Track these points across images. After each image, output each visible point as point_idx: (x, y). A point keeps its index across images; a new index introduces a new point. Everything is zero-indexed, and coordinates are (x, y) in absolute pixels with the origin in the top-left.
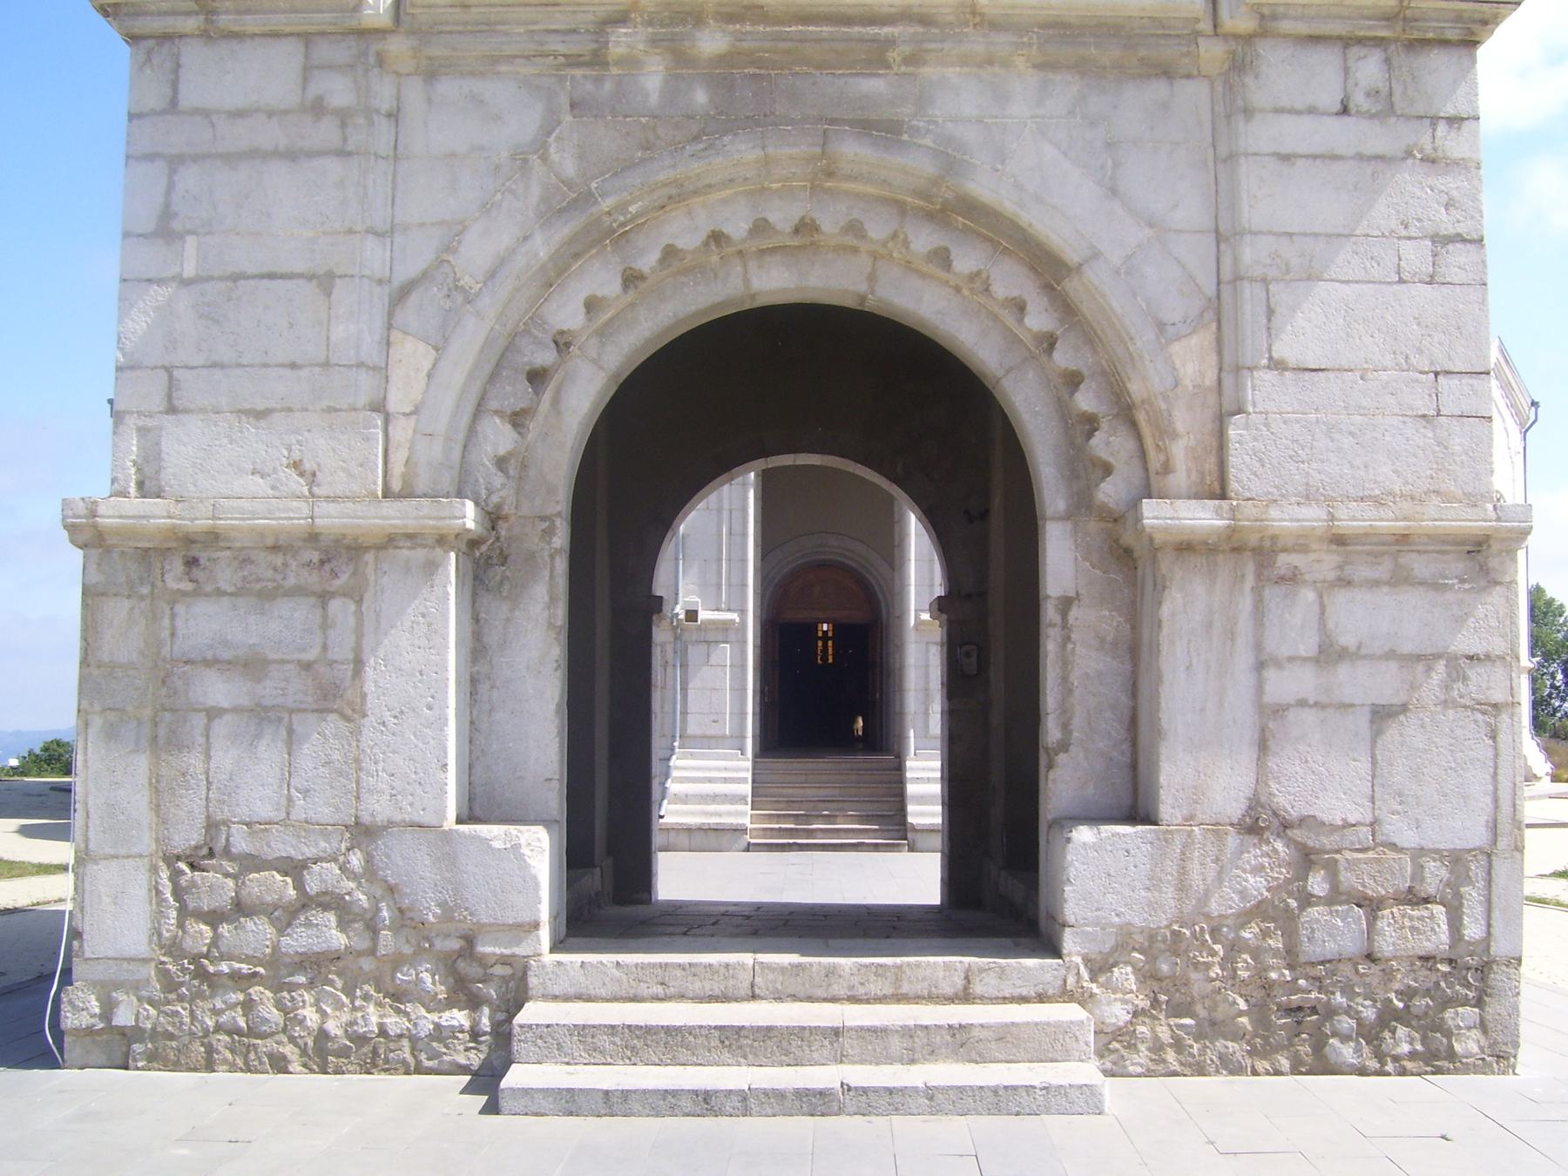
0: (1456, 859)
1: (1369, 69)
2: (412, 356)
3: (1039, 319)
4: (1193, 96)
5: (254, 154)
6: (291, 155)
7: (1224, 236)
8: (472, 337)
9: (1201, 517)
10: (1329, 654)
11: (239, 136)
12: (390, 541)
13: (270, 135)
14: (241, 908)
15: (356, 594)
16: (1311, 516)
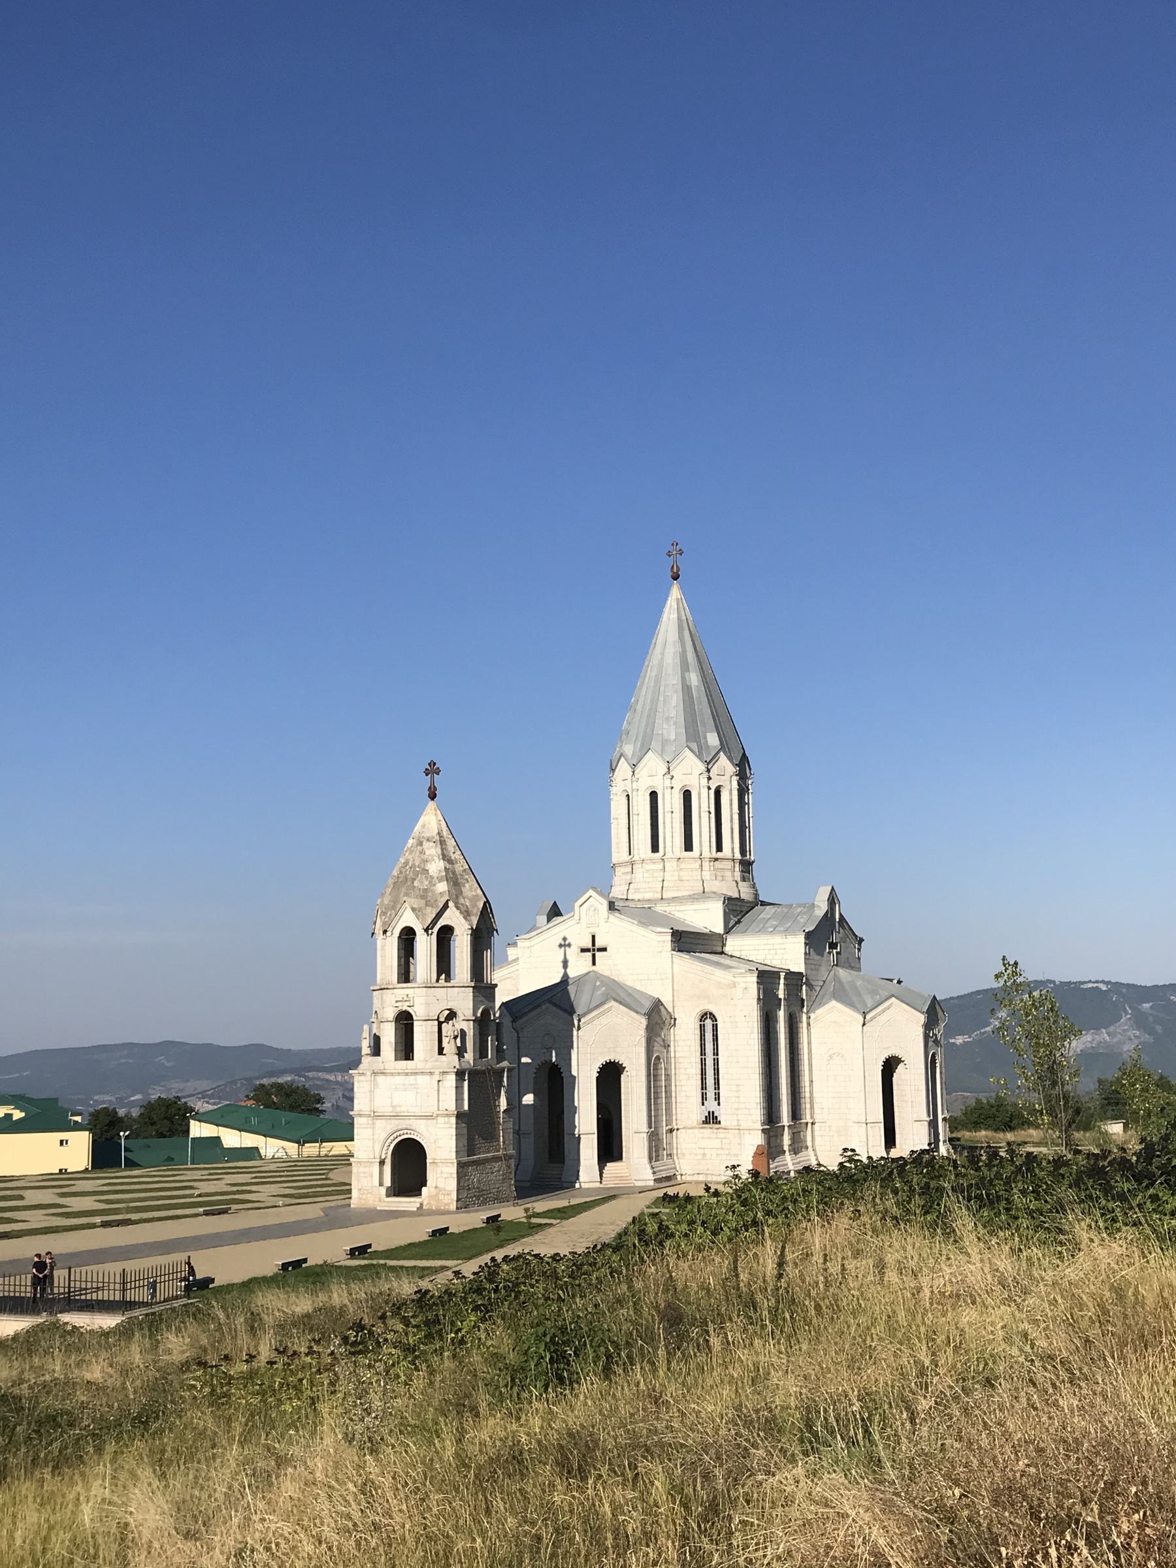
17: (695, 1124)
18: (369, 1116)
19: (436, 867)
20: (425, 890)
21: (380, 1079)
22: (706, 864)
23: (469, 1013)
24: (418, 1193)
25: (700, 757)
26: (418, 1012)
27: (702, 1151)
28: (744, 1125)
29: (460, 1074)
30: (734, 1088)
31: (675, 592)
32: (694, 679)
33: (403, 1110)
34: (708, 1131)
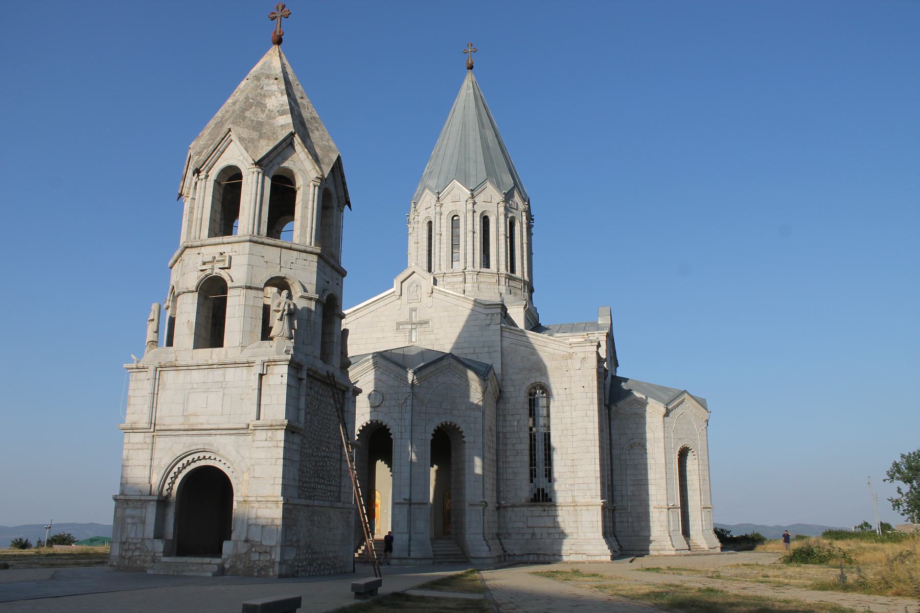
0: (271, 547)
1: (270, 433)
4: (250, 438)
8: (162, 472)
13: (140, 446)
16: (254, 499)
17: (523, 501)
19: (278, 100)
20: (260, 124)
21: (169, 377)
22: (503, 280)
23: (312, 291)
24: (218, 552)
25: (498, 186)
26: (236, 276)
27: (531, 531)
28: (581, 500)
29: (294, 366)
30: (569, 463)
31: (469, 81)
32: (490, 134)
33: (203, 421)
34: (537, 510)
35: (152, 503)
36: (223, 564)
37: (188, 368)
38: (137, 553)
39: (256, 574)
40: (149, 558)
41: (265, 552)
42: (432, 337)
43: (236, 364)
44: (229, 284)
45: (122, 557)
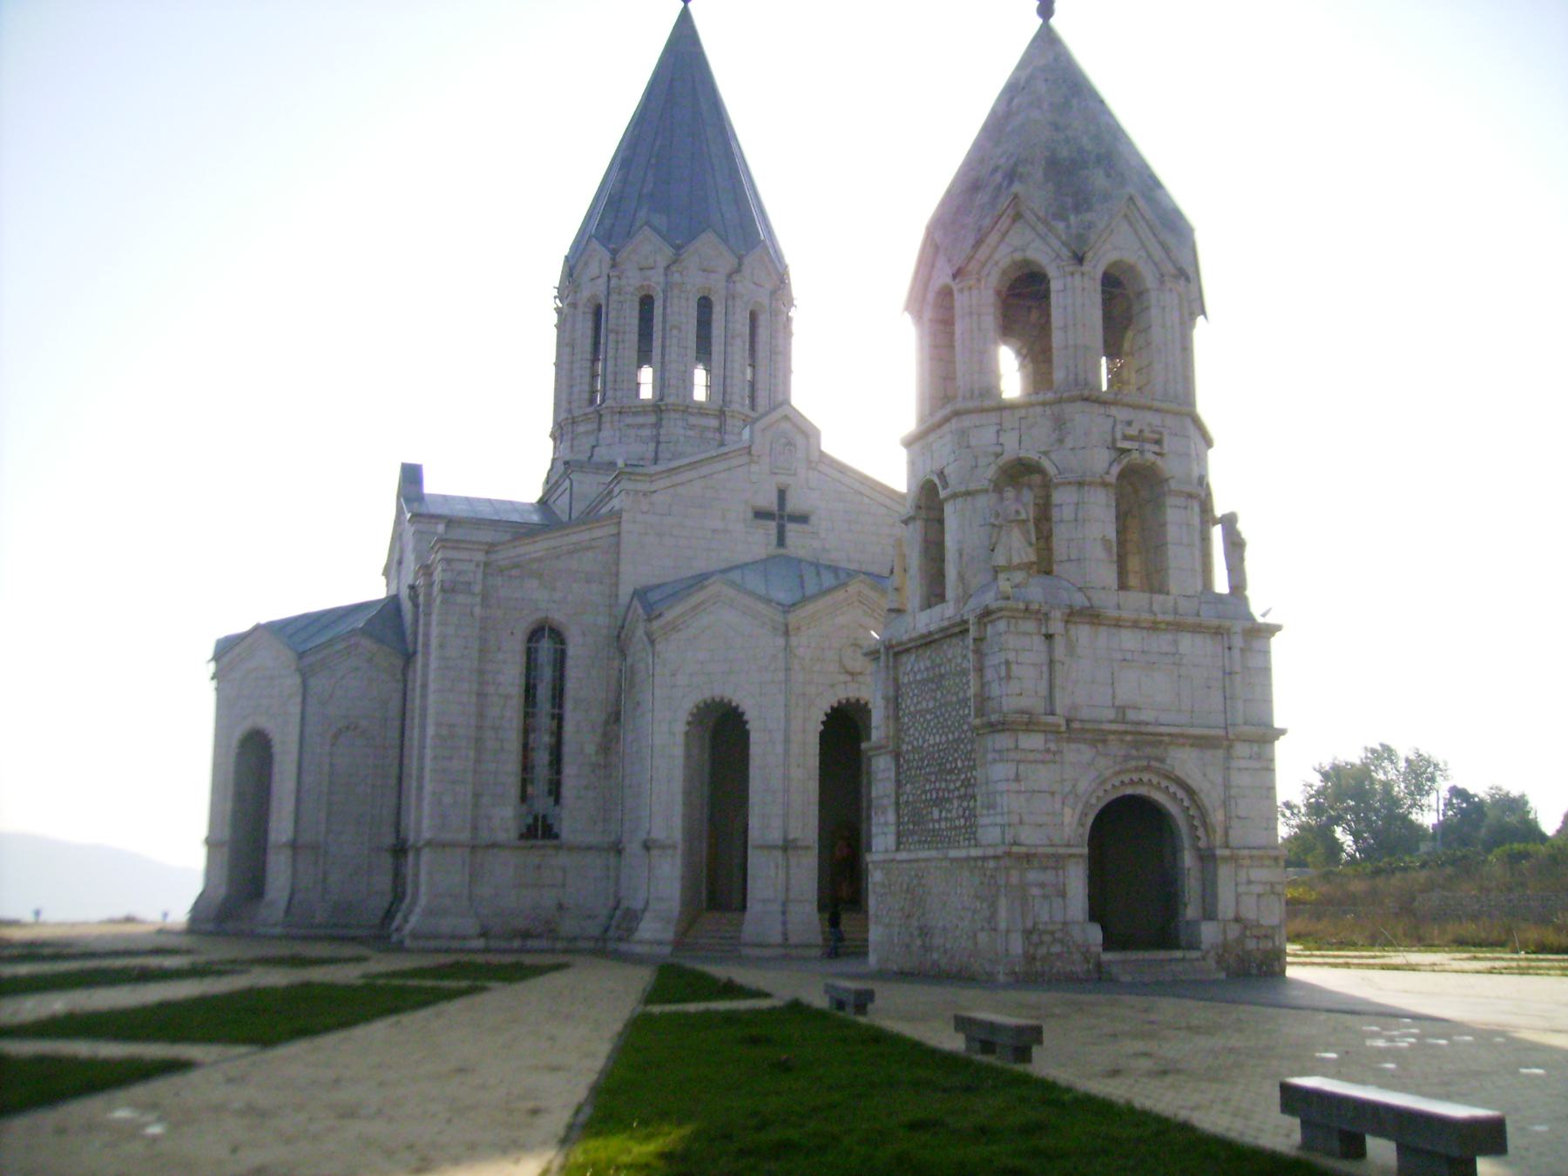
0: (1273, 928)
1: (1255, 748)
2: (1068, 811)
3: (1186, 803)
4: (1220, 753)
5: (1036, 761)
6: (1043, 762)
7: (1227, 786)
8: (1080, 806)
9: (1227, 852)
10: (1249, 882)
11: (1031, 756)
12: (1071, 856)
13: (1039, 756)
14: (1042, 943)
15: (1063, 868)
18: (1051, 731)
21: (1083, 633)
35: (1073, 860)
36: (1204, 958)
37: (1118, 624)
38: (1056, 949)
39: (1254, 971)
40: (1077, 957)
41: (1266, 936)
42: (816, 544)
43: (1197, 629)
44: (1173, 485)
45: (1030, 959)
